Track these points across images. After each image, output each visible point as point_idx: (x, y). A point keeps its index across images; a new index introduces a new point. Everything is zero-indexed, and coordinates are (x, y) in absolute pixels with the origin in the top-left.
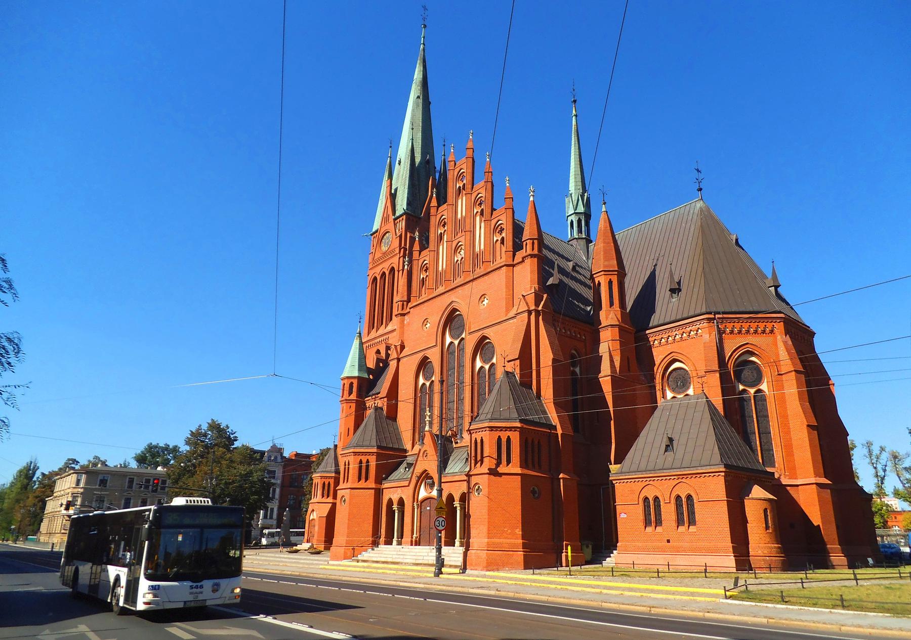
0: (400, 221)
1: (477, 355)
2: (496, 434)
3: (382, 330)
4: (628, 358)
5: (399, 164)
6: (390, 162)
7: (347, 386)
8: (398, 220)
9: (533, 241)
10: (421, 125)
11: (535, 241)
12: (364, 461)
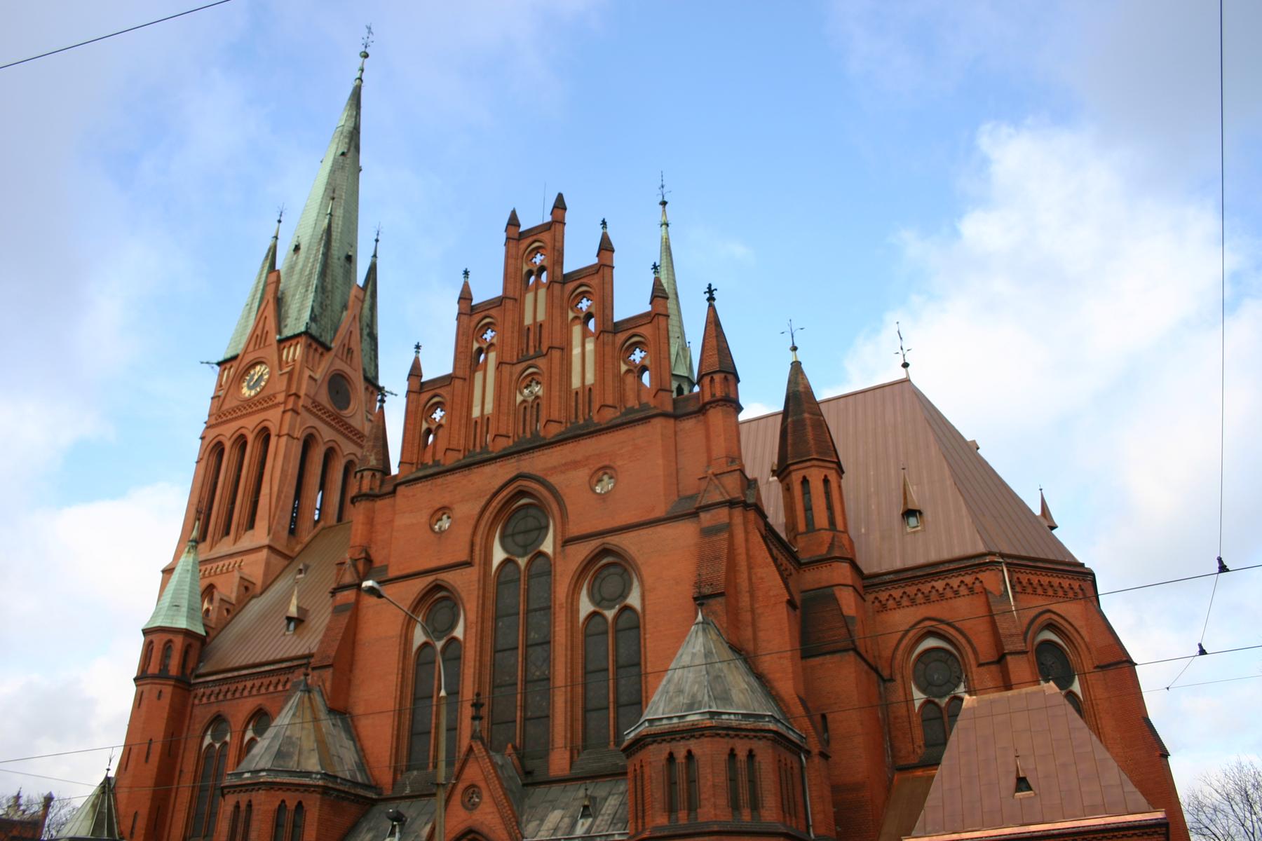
0: (291, 346)
1: (581, 589)
3: (225, 547)
7: (158, 647)
8: (287, 344)
9: (712, 378)
11: (377, 474)
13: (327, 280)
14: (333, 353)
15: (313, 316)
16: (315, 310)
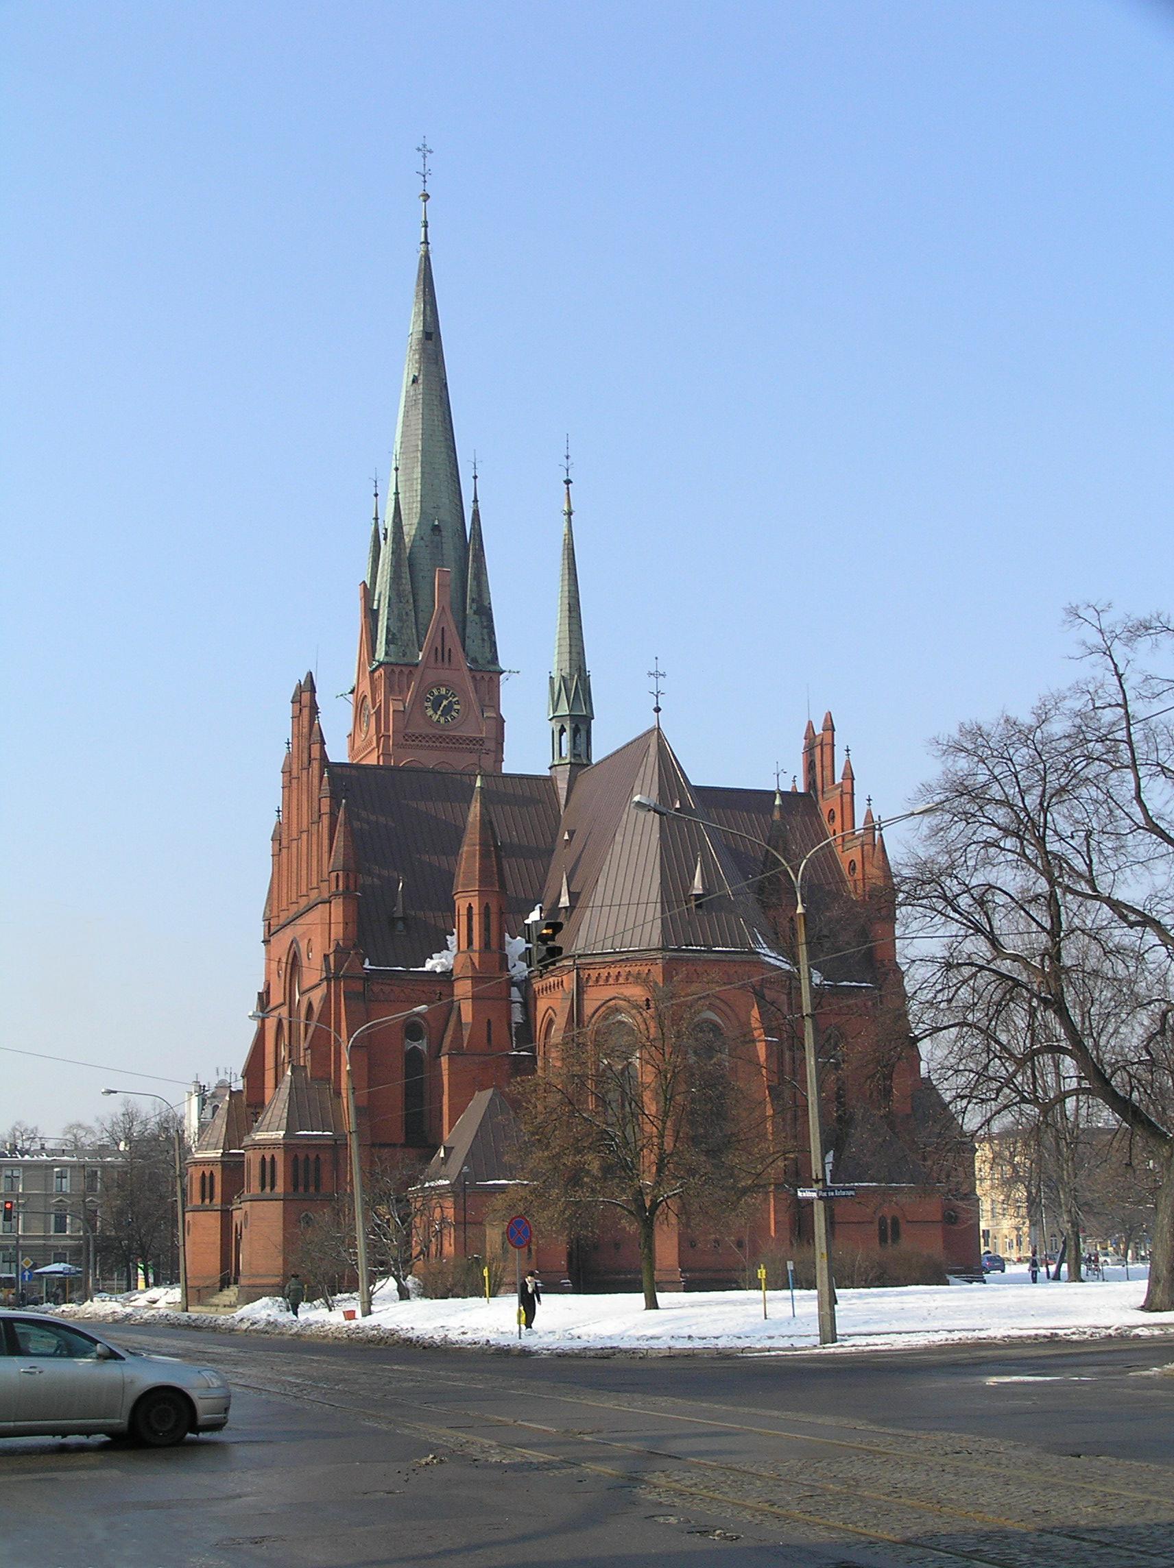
2: (260, 1153)
4: (489, 1022)
5: (385, 539)
6: (377, 530)
10: (420, 448)
12: (301, 1157)
13: (404, 581)
14: (421, 668)
15: (390, 637)
16: (392, 629)
